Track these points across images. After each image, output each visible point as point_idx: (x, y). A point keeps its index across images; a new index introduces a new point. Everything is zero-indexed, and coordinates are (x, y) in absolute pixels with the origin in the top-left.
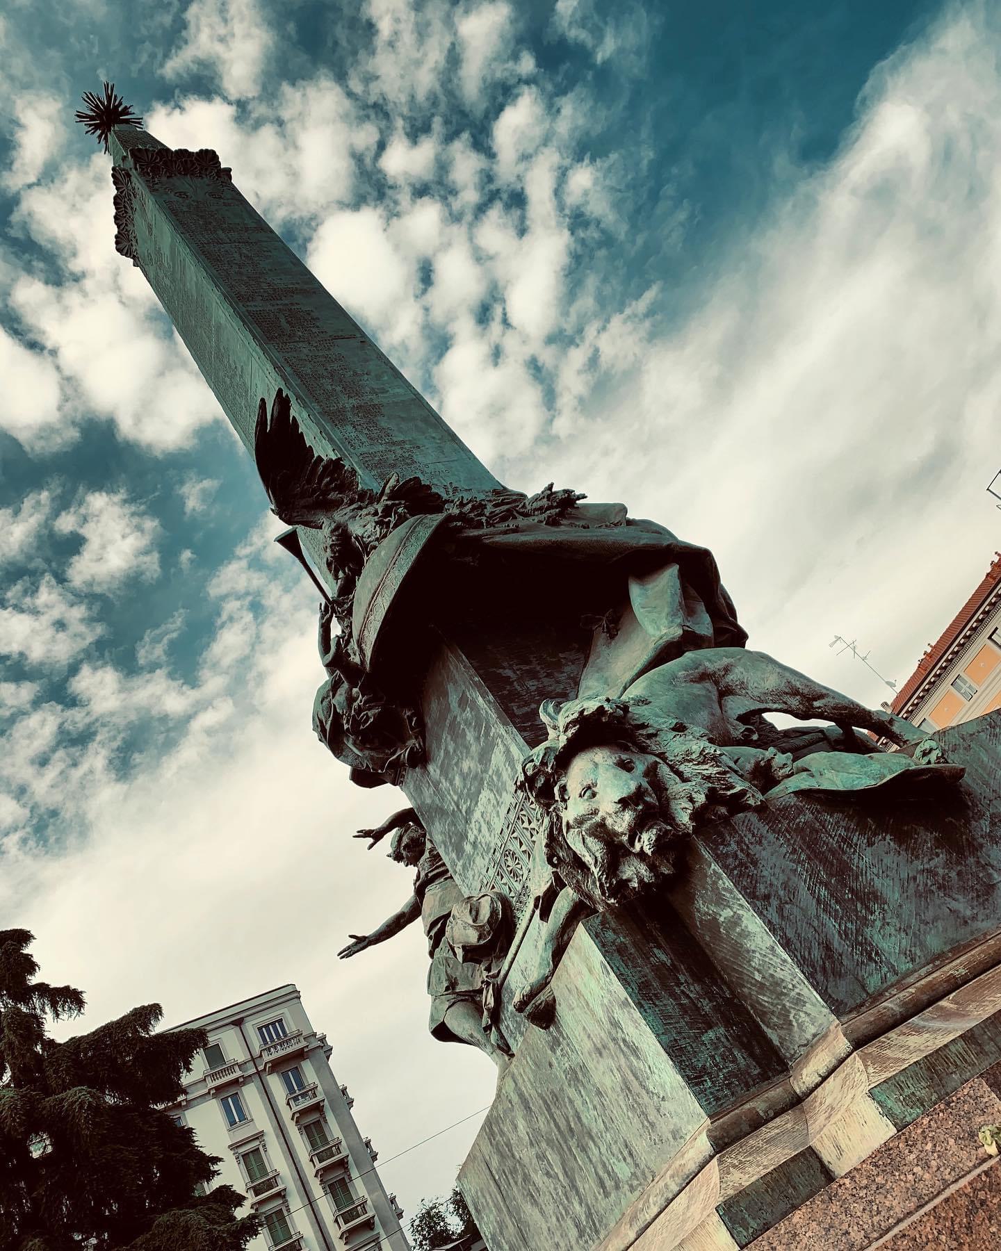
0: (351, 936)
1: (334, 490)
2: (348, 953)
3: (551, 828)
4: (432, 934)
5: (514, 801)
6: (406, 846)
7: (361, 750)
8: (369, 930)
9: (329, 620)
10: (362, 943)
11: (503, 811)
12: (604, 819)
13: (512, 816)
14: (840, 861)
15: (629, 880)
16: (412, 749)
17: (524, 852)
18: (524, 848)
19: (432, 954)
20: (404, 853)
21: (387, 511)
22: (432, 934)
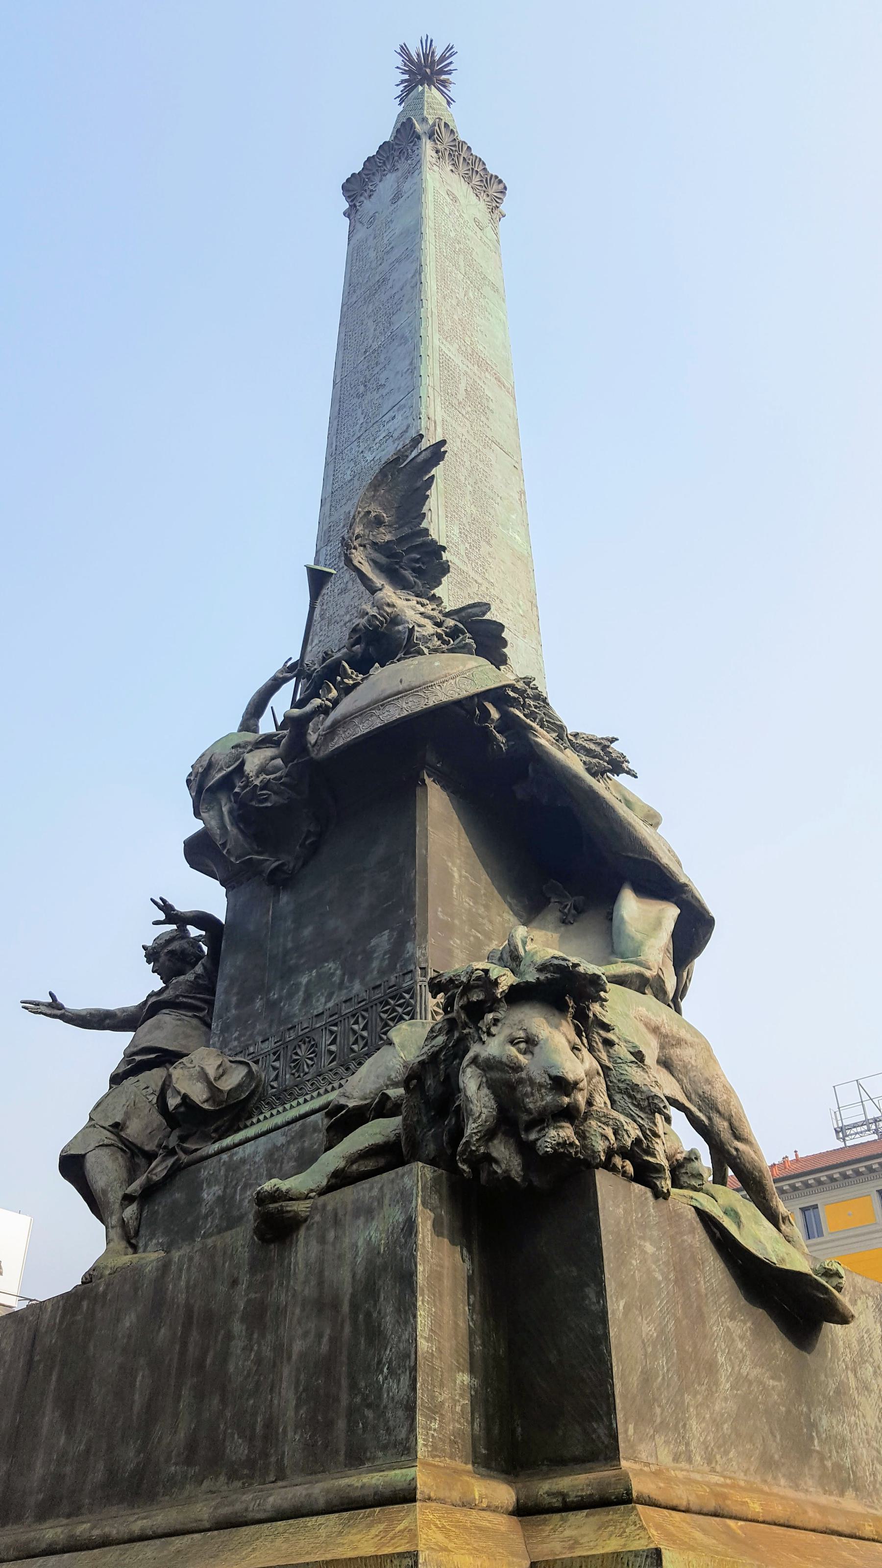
0: (51, 994)
1: (414, 570)
2: (34, 1007)
3: (441, 1050)
4: (138, 1058)
5: (364, 995)
6: (172, 953)
7: (232, 824)
8: (72, 1003)
9: (286, 680)
10: (54, 1009)
11: (344, 995)
12: (521, 1081)
13: (346, 1010)
14: (699, 1309)
15: (496, 1161)
16: (283, 864)
17: (331, 1052)
18: (333, 1048)
19: (116, 1079)
20: (163, 958)
21: (454, 633)
22: (138, 1058)
